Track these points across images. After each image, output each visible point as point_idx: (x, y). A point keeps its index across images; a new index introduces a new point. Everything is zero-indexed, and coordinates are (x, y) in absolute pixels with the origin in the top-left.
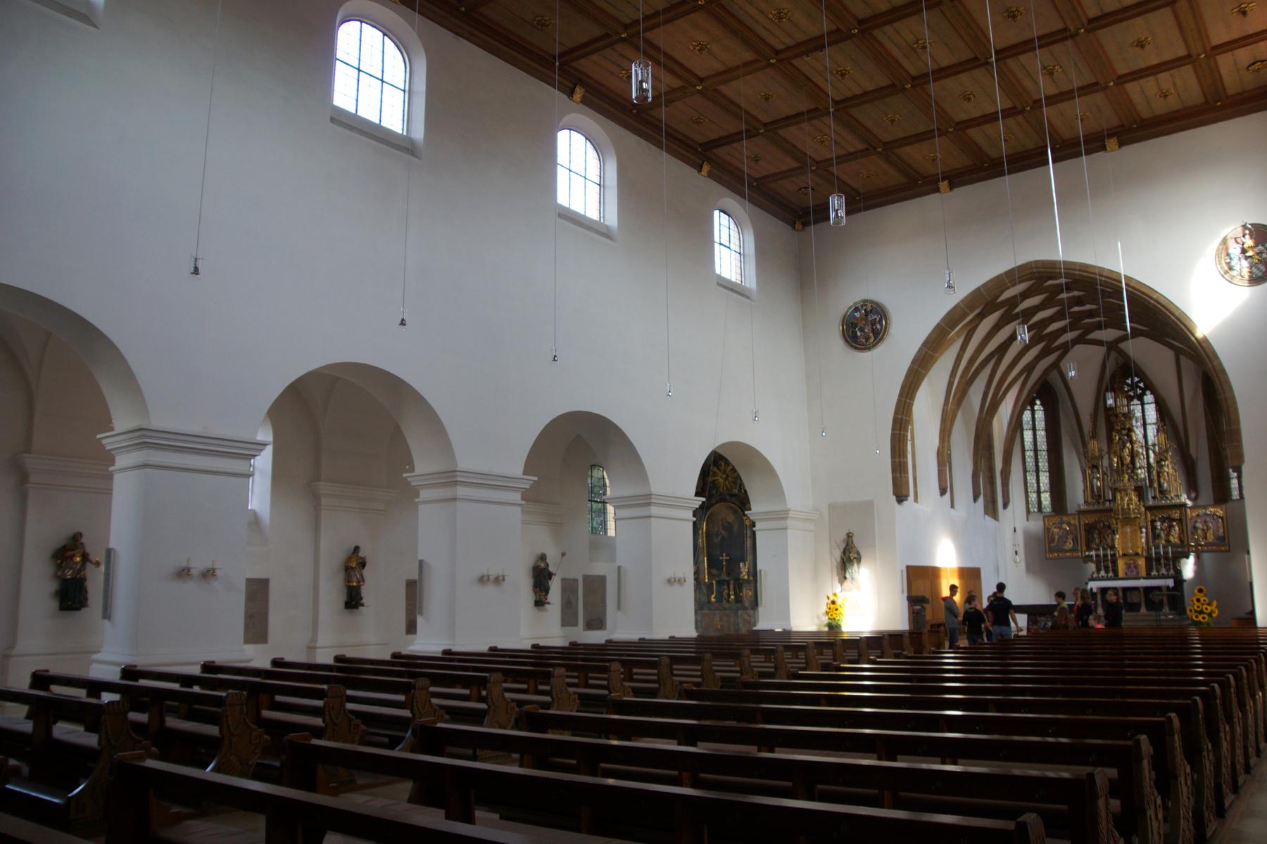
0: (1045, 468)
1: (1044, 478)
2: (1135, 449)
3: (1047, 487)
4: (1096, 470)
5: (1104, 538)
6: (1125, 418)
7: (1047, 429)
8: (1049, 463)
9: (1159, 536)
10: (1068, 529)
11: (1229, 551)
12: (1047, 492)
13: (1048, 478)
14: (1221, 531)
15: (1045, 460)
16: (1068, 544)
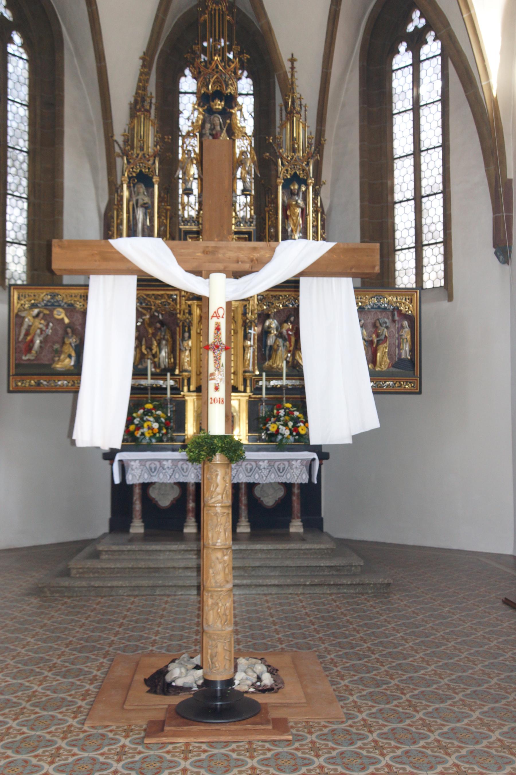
0: (21, 189)
1: (17, 211)
2: (238, 151)
3: (22, 234)
4: (142, 188)
5: (149, 348)
6: (224, 68)
7: (31, 106)
8: (29, 179)
9: (273, 350)
10: (67, 321)
11: (420, 393)
12: (19, 244)
13: (25, 214)
14: (407, 347)
15: (21, 172)
16: (62, 357)
